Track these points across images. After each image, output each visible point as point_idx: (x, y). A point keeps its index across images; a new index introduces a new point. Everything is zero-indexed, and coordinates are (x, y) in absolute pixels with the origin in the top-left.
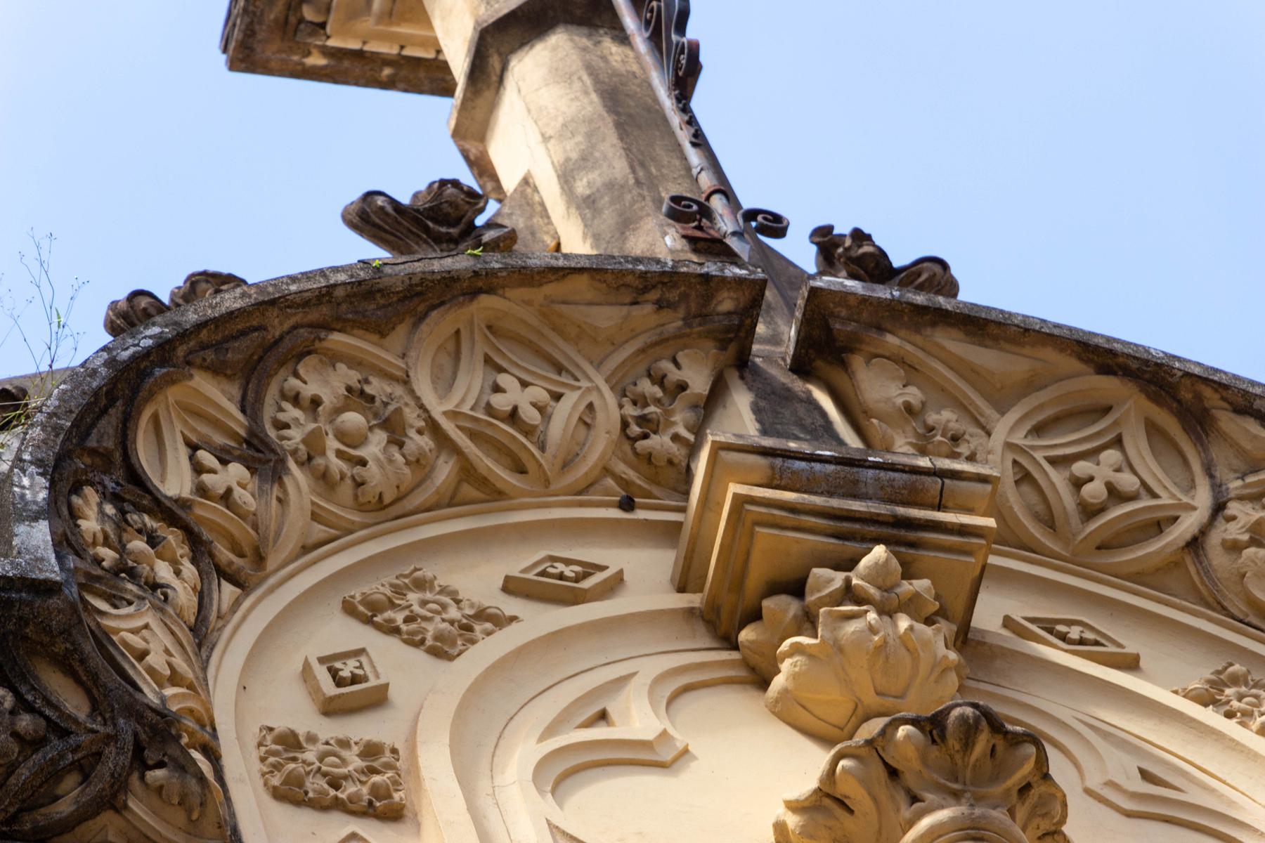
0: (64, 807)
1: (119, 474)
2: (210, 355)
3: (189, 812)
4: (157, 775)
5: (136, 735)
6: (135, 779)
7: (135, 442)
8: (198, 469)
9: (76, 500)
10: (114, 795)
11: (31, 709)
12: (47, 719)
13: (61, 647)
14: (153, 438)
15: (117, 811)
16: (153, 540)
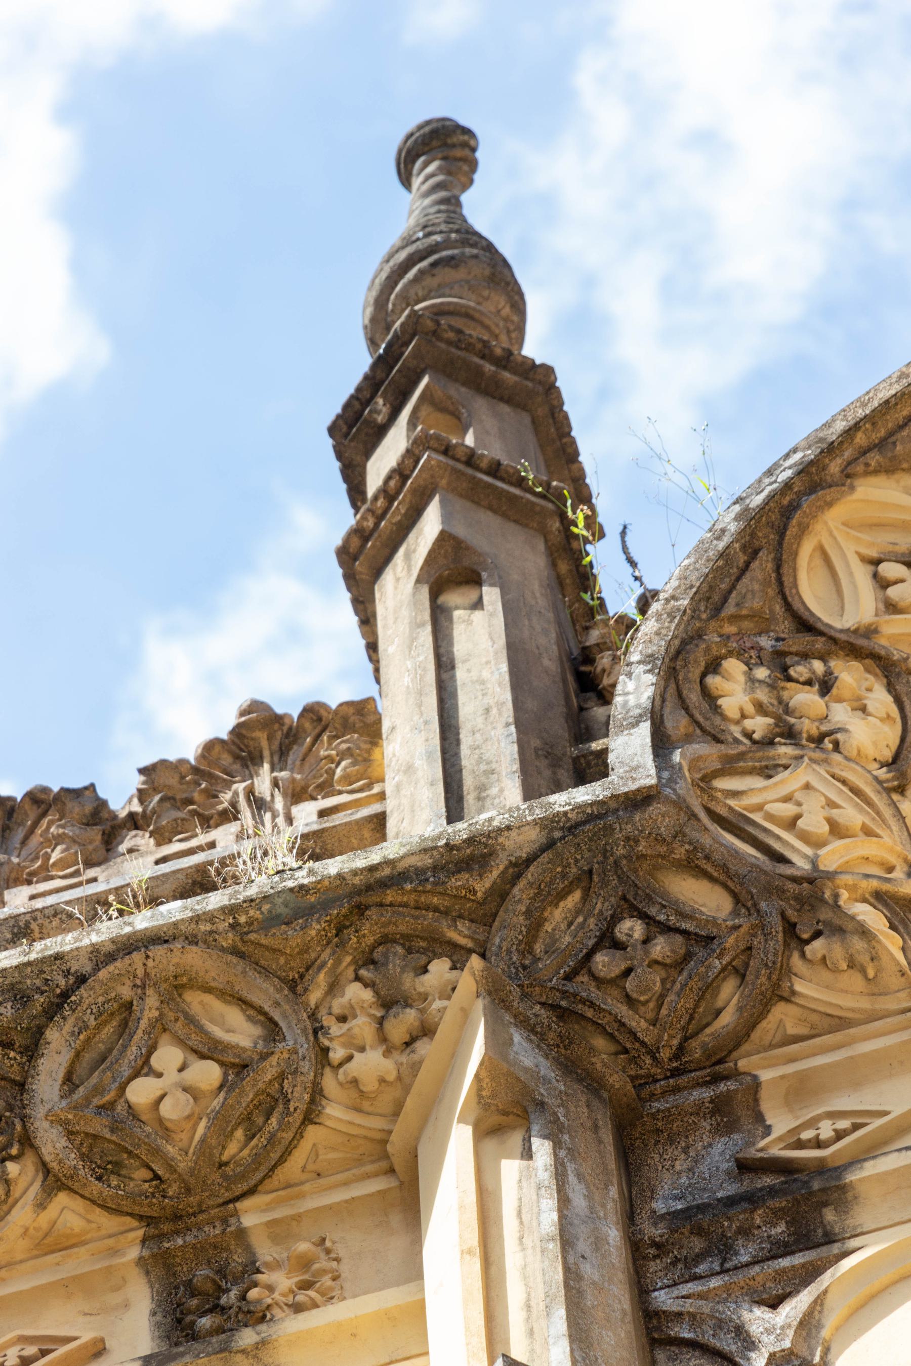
0: (727, 1018)
1: (784, 626)
2: (874, 459)
3: (863, 971)
4: (817, 947)
5: (783, 915)
6: (796, 960)
7: (795, 585)
8: (883, 584)
9: (713, 681)
10: (777, 986)
11: (667, 929)
12: (684, 933)
13: (680, 852)
14: (822, 572)
15: (787, 1001)
16: (826, 686)
